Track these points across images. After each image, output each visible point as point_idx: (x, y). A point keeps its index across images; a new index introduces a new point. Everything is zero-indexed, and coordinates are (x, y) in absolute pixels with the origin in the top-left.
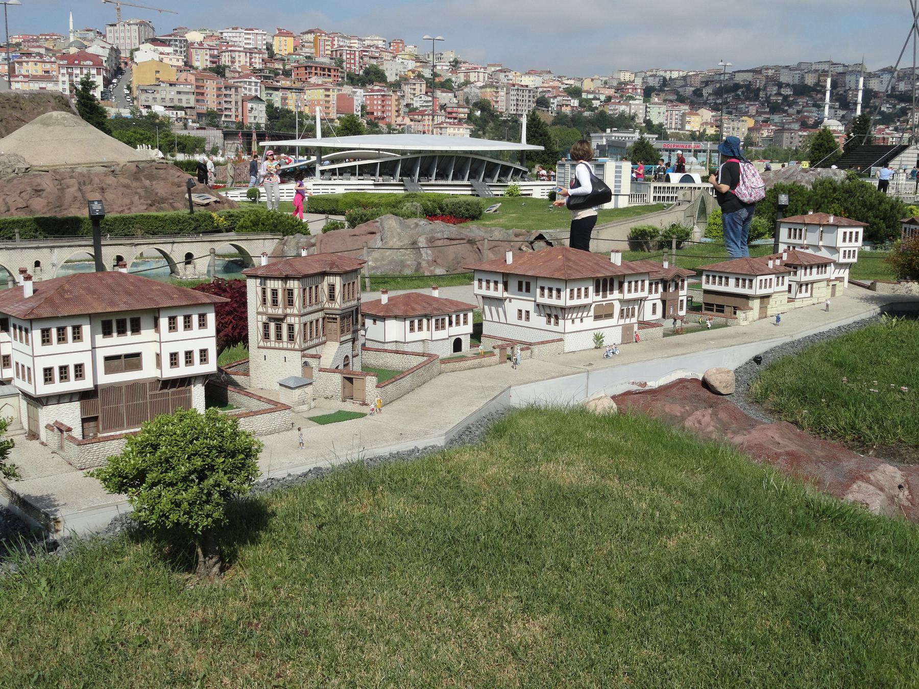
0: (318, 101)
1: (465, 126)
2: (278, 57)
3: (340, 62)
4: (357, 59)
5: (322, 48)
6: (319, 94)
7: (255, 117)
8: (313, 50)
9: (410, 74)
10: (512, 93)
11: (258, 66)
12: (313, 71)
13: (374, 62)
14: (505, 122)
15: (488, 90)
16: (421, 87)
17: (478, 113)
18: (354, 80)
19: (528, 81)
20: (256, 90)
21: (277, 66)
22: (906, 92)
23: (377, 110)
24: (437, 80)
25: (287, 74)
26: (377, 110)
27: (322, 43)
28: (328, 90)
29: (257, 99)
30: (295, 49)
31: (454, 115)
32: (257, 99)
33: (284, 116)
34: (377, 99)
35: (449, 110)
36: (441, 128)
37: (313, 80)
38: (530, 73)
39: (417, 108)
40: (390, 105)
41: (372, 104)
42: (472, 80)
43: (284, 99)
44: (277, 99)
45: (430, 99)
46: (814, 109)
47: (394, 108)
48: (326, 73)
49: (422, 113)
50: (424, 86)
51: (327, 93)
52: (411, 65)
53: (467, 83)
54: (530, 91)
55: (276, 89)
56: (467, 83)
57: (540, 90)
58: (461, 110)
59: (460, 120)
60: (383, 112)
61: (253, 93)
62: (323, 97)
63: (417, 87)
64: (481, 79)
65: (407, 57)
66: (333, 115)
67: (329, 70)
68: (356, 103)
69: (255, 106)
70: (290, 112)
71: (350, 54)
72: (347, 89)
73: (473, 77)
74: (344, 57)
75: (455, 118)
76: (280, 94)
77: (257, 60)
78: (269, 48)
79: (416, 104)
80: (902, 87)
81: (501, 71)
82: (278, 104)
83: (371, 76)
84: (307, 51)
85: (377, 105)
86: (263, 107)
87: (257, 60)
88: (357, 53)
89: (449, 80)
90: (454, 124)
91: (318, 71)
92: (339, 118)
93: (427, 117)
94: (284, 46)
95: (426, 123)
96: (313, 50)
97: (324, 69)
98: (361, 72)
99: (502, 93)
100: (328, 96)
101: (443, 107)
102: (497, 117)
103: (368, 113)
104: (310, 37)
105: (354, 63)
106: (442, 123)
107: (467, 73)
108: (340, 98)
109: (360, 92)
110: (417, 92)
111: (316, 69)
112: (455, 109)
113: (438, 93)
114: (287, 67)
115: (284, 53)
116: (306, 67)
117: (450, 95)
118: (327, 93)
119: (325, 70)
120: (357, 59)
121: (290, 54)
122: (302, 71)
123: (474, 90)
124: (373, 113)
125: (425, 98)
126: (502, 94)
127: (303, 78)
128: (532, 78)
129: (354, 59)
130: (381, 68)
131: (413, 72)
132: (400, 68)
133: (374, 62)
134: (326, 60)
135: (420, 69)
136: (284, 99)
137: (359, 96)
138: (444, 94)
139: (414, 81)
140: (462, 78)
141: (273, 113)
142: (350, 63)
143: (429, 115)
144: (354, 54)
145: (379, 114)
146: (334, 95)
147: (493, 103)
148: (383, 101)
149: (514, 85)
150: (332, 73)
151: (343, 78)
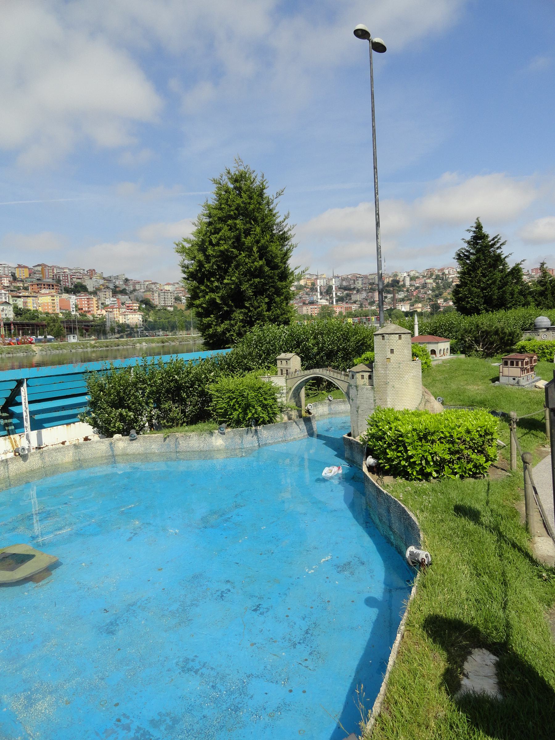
0: (48, 303)
1: (139, 313)
2: (19, 279)
3: (59, 281)
4: (69, 279)
5: (47, 273)
6: (48, 299)
7: (6, 314)
8: (41, 276)
9: (101, 287)
10: (161, 294)
11: (6, 285)
12: (43, 286)
13: (79, 281)
14: (159, 310)
15: (148, 293)
16: (109, 293)
17: (144, 306)
18: (67, 291)
19: (167, 288)
20: (6, 298)
21: (19, 285)
22: (347, 286)
23: (85, 307)
24: (117, 289)
25: (26, 289)
26: (85, 307)
27: (46, 271)
28: (53, 296)
29: (7, 303)
30: (30, 275)
31: (131, 308)
32: (7, 303)
33: (25, 313)
34: (84, 301)
35: (127, 305)
36: (125, 315)
37: (43, 291)
38: (168, 284)
39: (108, 305)
40: (93, 304)
41: (82, 304)
42: (137, 288)
43: (25, 303)
44: (20, 303)
45: (115, 299)
46: (307, 296)
47: (95, 305)
48: (51, 287)
49: (113, 308)
50: (111, 293)
51: (53, 298)
52: (102, 282)
53: (135, 290)
54: (171, 293)
55: (19, 297)
56: (135, 290)
57: (176, 292)
58: (134, 305)
59: (135, 310)
60: (89, 308)
61: (4, 300)
62: (50, 301)
63: (107, 293)
64: (142, 288)
65: (98, 278)
66: (58, 311)
67: (53, 286)
68: (71, 303)
69: (5, 308)
70: (29, 310)
71: (65, 277)
72: (65, 296)
73: (138, 287)
74: (61, 278)
75: (131, 309)
76: (22, 299)
77: (5, 281)
78: (13, 275)
79: (108, 302)
80: (345, 284)
81: (152, 283)
82: (20, 305)
83: (78, 289)
84: (38, 276)
85: (85, 304)
86: (11, 308)
87: (5, 281)
88: (69, 276)
89: (125, 289)
90: (132, 312)
91: (46, 287)
92: (61, 313)
93: (115, 309)
94: (22, 274)
95: (115, 312)
96: (41, 276)
97: (49, 285)
98: (72, 287)
99: (156, 294)
100: (54, 300)
101: (123, 304)
102: (155, 307)
103: (79, 309)
104: (39, 268)
105: (68, 282)
106: (125, 312)
107: (134, 286)
108: (61, 301)
109: (73, 297)
110: (107, 296)
111: (44, 285)
112: (131, 305)
113: (120, 296)
114: (25, 285)
115: (22, 277)
116: (38, 285)
117: (127, 297)
118: (53, 298)
119: (50, 286)
120: (69, 279)
121: (27, 278)
122: (36, 287)
123: (140, 293)
124: (82, 309)
125: (112, 299)
126: (156, 295)
127: (37, 291)
128: (170, 287)
129: (68, 279)
130: (84, 284)
131: (103, 285)
132: (96, 284)
133: (79, 281)
134: (51, 280)
135: (107, 284)
136: (25, 303)
137: (73, 299)
138: (123, 297)
139: (105, 290)
140: (132, 288)
141: (18, 312)
142: (65, 282)
143: (116, 308)
144: (67, 277)
145: (86, 309)
146: (57, 299)
147: (151, 300)
148: (88, 302)
149: (162, 290)
150: (55, 287)
151: (61, 290)
